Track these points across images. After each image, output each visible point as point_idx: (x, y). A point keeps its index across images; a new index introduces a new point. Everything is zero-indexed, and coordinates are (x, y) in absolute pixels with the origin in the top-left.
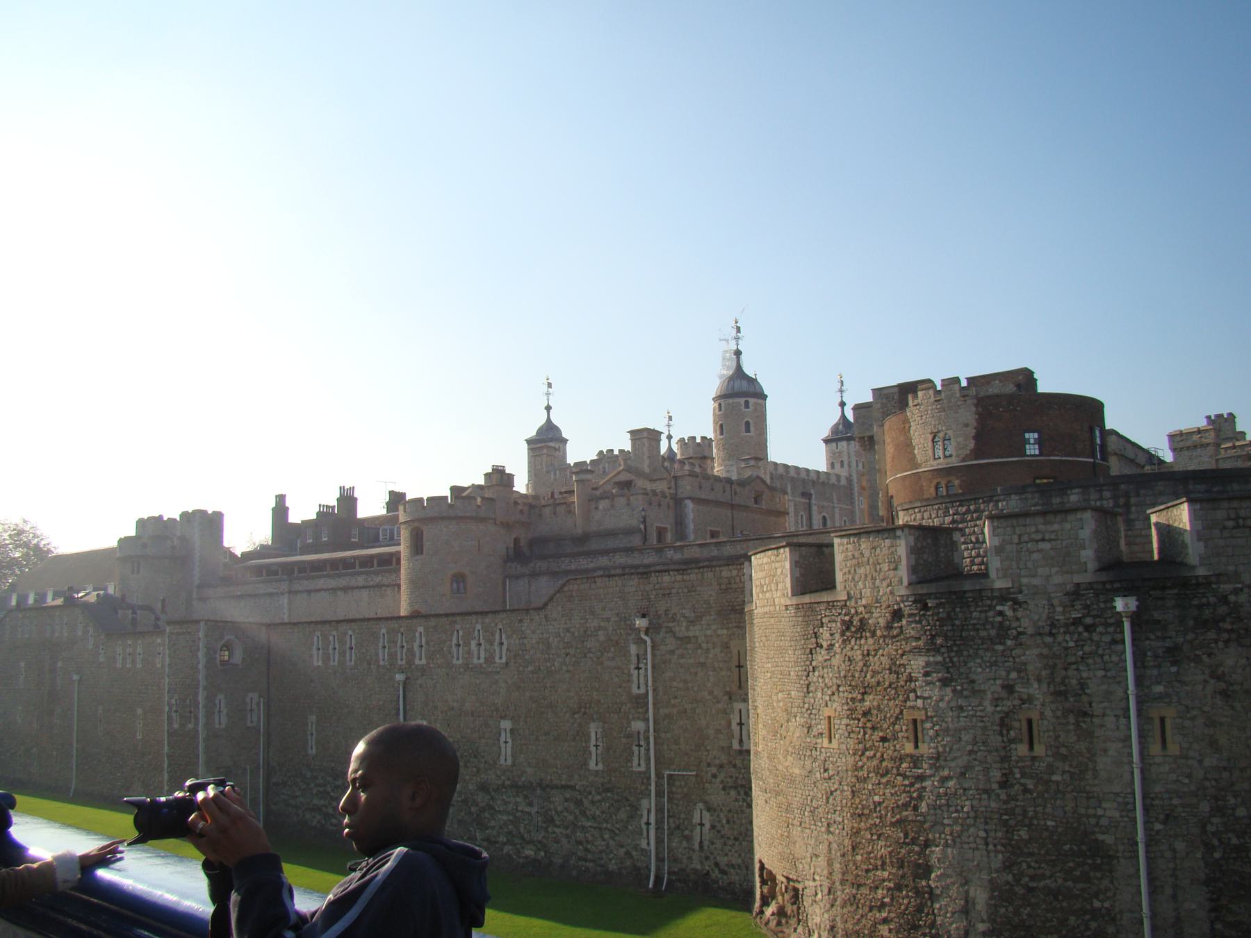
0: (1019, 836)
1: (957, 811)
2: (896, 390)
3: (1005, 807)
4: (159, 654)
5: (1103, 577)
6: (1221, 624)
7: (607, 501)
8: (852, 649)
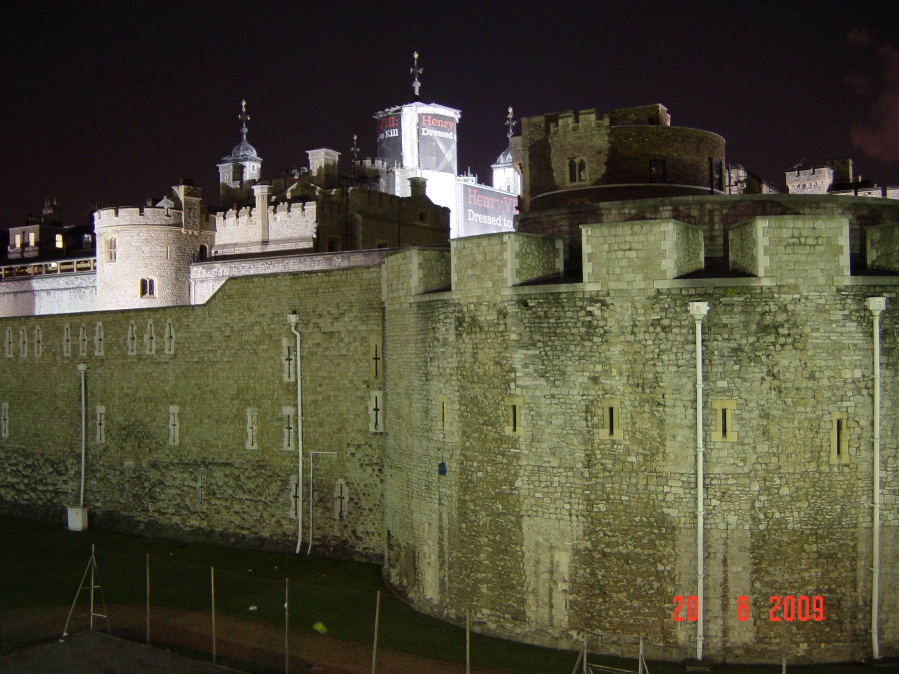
0: (599, 508)
1: (547, 486)
3: (587, 483)
5: (681, 283)
6: (780, 330)
8: (464, 342)
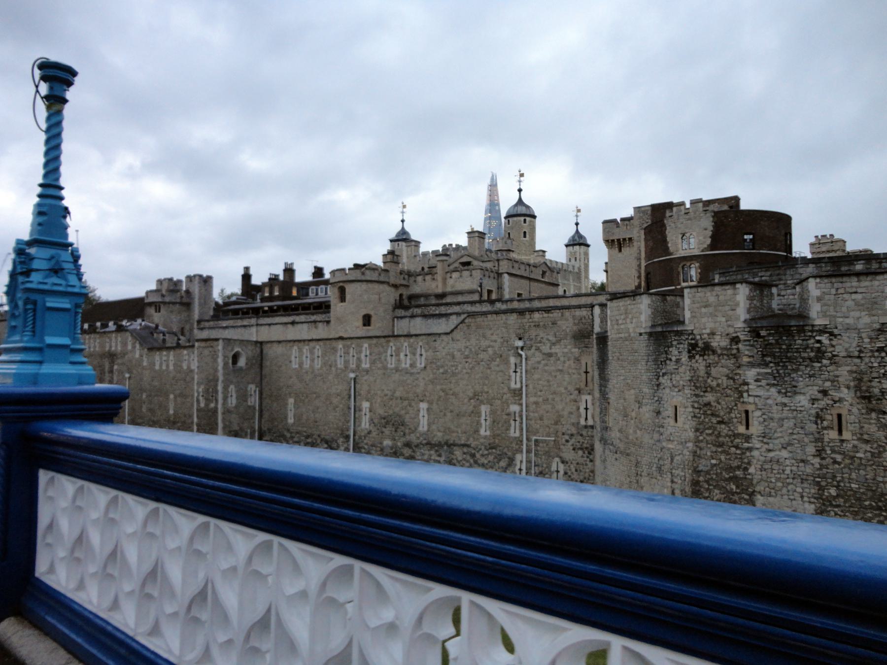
0: (830, 493)
1: (778, 473)
2: (649, 208)
4: (185, 360)
7: (458, 273)
8: (697, 362)
